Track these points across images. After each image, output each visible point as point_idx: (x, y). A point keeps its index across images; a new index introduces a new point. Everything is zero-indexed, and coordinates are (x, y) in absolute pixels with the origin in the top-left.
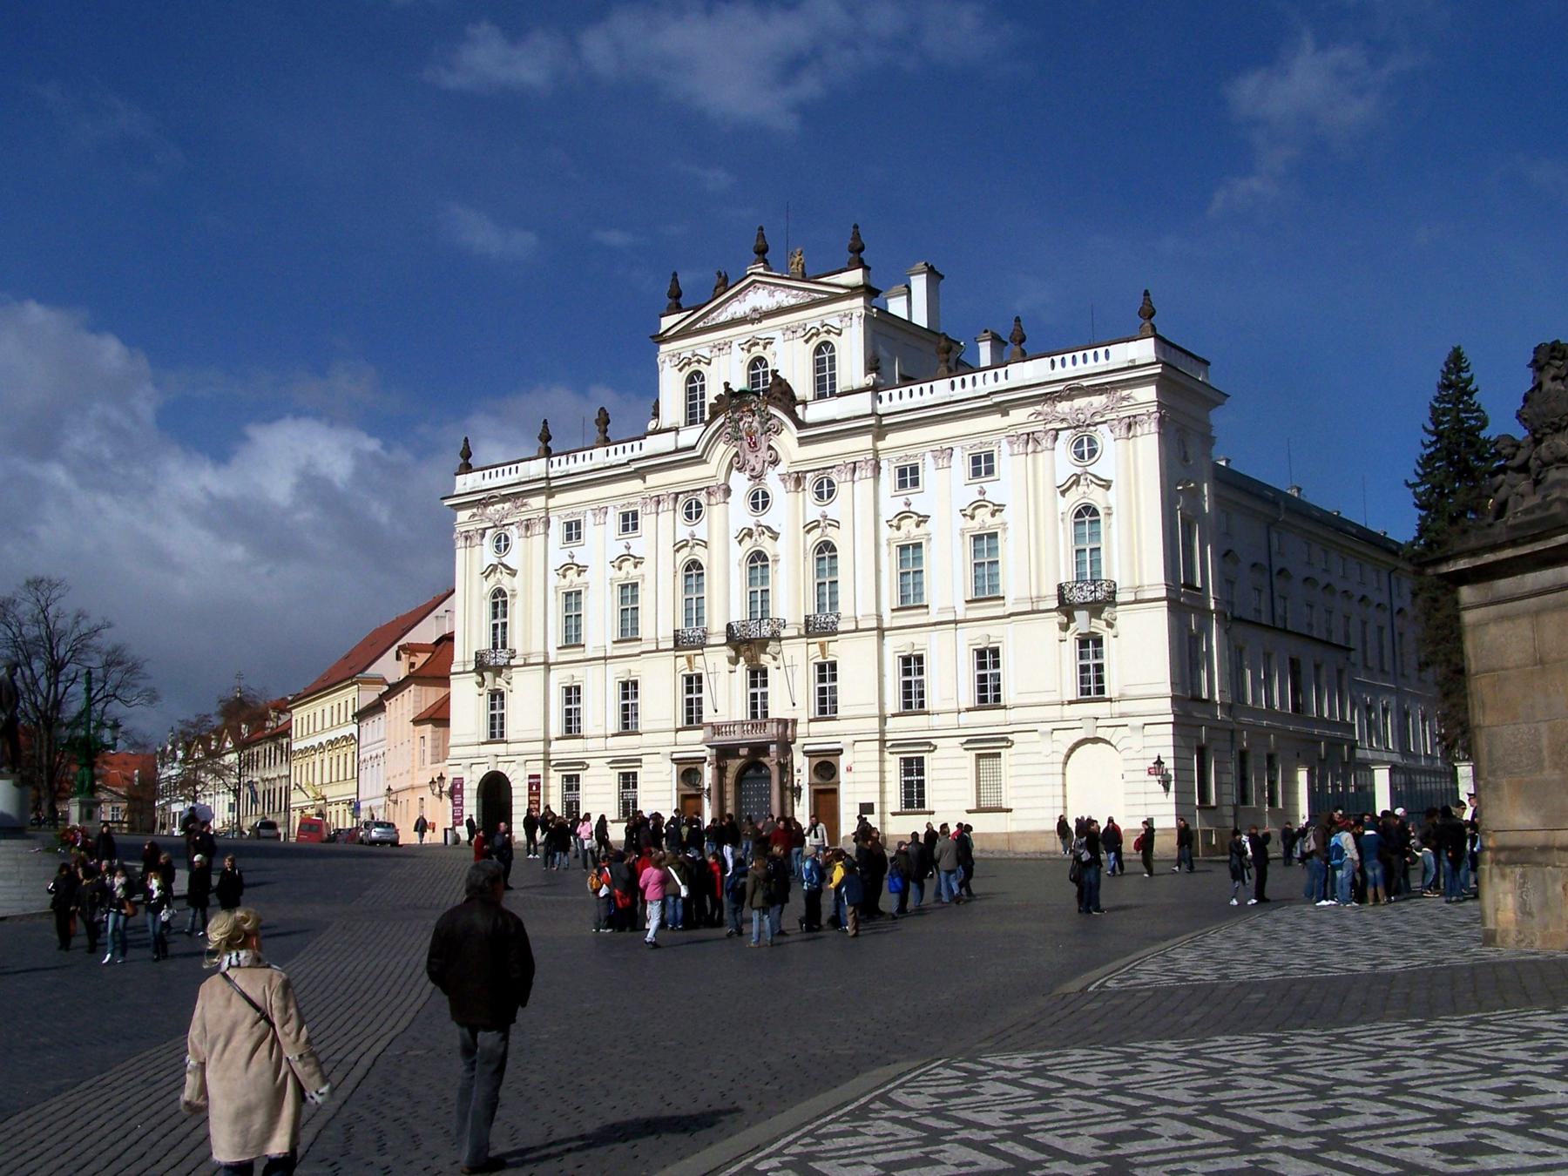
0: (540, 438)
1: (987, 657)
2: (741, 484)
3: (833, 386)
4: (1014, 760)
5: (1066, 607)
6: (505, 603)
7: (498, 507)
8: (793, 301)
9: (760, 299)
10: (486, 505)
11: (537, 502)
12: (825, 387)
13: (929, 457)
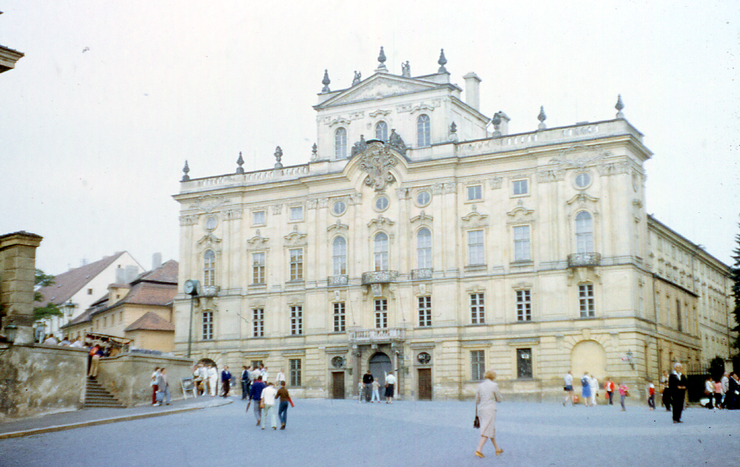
0: (238, 162)
1: (523, 295)
2: (370, 192)
3: (428, 140)
4: (538, 352)
5: (572, 267)
8: (403, 91)
9: (384, 88)
10: (201, 201)
11: (237, 200)
12: (425, 138)
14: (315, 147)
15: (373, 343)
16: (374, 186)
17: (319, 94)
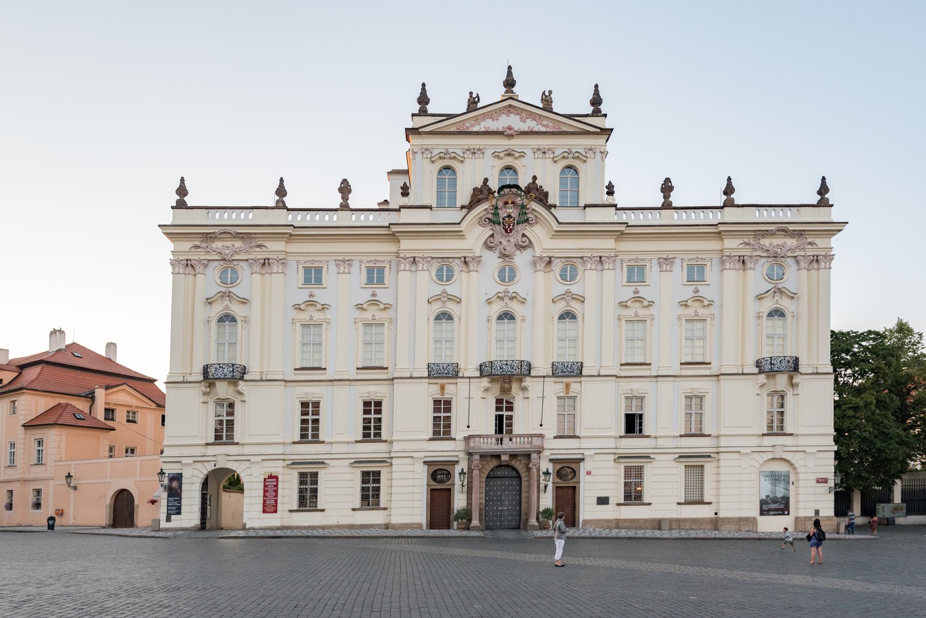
9: (514, 122)
13: (655, 262)
16: (497, 252)
17: (413, 115)
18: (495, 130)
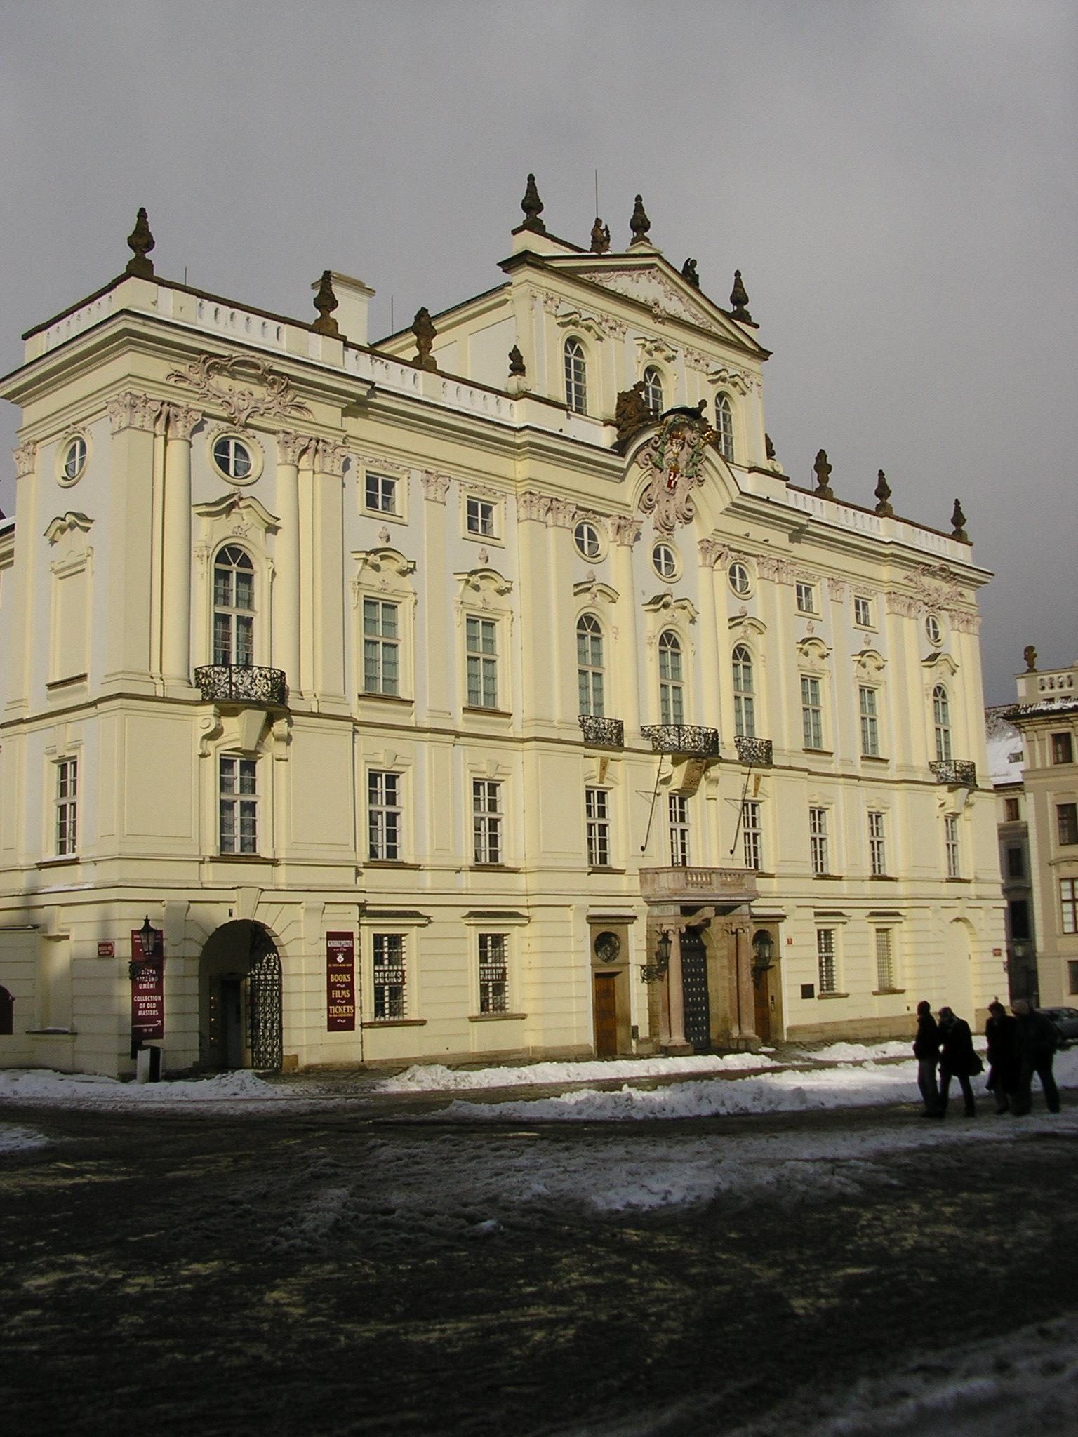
6: (246, 579)
7: (240, 386)
8: (693, 321)
14: (515, 356)
15: (710, 903)
18: (634, 297)
